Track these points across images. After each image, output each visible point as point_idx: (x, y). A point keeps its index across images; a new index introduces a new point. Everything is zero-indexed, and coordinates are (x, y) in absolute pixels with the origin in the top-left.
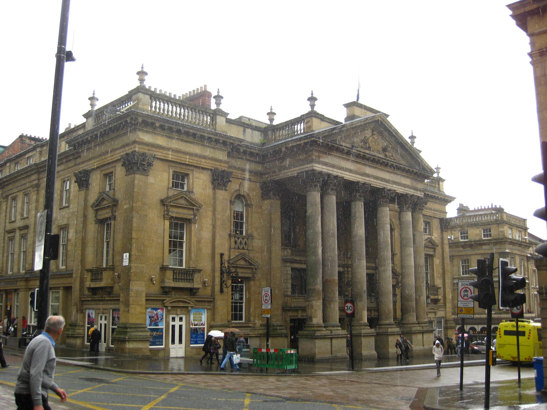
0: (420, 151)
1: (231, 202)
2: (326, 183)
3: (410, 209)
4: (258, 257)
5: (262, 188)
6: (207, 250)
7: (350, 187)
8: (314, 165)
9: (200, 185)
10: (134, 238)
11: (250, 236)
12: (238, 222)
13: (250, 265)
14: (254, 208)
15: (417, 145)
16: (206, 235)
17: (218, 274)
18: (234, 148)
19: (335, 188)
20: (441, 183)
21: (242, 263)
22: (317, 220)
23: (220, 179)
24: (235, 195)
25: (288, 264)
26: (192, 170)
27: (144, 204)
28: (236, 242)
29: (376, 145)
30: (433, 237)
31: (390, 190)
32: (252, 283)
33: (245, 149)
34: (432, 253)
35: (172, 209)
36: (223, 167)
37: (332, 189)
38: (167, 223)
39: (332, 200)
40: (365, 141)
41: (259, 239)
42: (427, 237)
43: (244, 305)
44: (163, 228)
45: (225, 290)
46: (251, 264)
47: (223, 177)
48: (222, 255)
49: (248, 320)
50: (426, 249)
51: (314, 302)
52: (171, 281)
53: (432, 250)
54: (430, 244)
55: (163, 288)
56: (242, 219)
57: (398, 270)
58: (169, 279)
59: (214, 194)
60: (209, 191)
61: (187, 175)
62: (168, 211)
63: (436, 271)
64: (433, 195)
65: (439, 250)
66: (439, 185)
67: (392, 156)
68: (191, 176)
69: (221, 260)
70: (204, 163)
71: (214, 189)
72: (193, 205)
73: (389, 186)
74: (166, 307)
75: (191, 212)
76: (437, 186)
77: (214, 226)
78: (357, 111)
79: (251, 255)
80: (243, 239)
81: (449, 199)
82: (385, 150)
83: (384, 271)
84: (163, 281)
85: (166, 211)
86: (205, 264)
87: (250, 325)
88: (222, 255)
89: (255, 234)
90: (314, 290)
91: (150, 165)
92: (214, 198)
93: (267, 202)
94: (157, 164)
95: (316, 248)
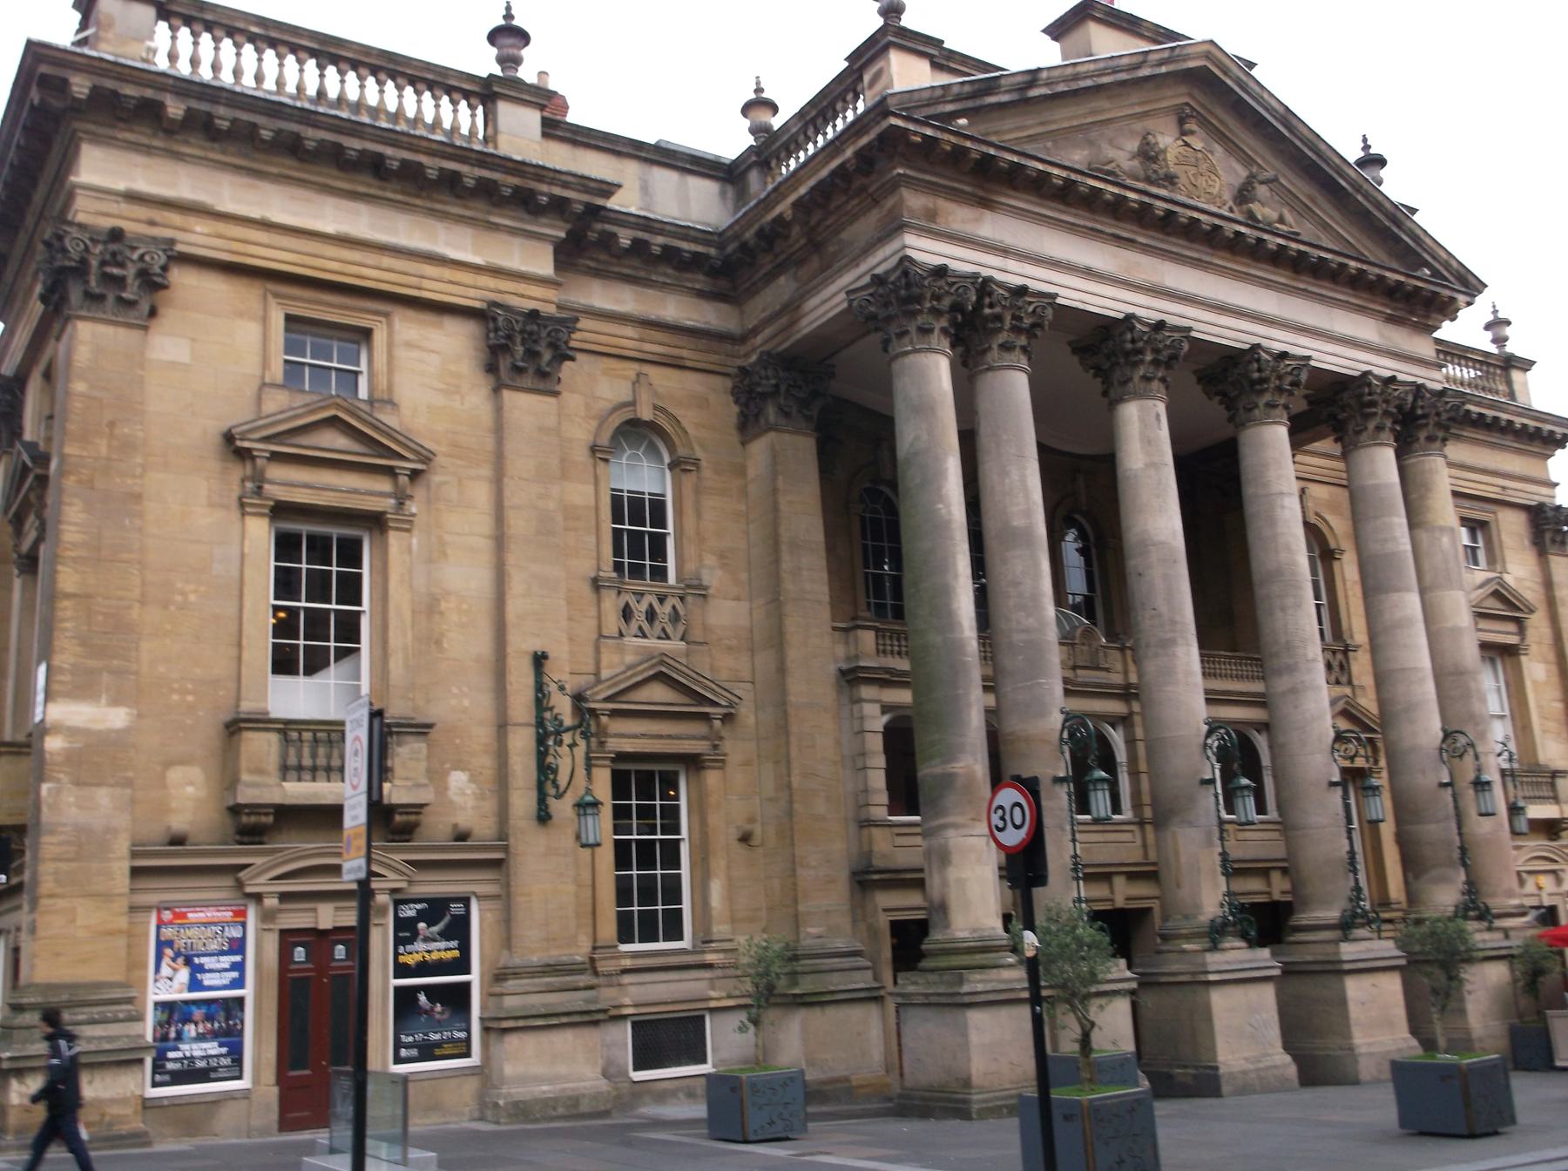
0: (1414, 211)
1: (593, 449)
2: (978, 321)
3: (1387, 436)
4: (724, 667)
5: (736, 393)
6: (467, 642)
7: (1103, 353)
8: (910, 239)
9: (425, 375)
10: (68, 596)
11: (695, 589)
12: (637, 535)
13: (697, 703)
14: (707, 472)
15: (1395, 186)
16: (466, 577)
17: (522, 742)
18: (589, 235)
19: (1023, 341)
20: (1516, 375)
21: (658, 694)
22: (940, 474)
23: (522, 349)
24: (616, 420)
25: (867, 692)
26: (386, 315)
27: (127, 447)
28: (627, 613)
29: (1210, 179)
30: (1508, 579)
31: (1284, 355)
32: (712, 778)
33: (640, 235)
34: (1513, 640)
35: (276, 472)
36: (541, 300)
37: (1007, 347)
38: (261, 534)
39: (1013, 390)
40: (1148, 154)
41: (737, 599)
42: (1480, 575)
43: (685, 871)
44: (235, 551)
45: (554, 805)
46: (702, 700)
47: (530, 338)
48: (539, 660)
49: (705, 940)
50: (1483, 624)
51: (951, 833)
52: (273, 779)
53: (1512, 627)
54: (1499, 606)
55: (235, 810)
56: (659, 520)
57: (1368, 702)
58: (260, 771)
59: (499, 410)
60: (475, 397)
61: (366, 334)
62: (259, 480)
63: (1540, 707)
64: (1490, 413)
65: (1538, 625)
66: (1509, 383)
67: (1281, 220)
68: (379, 337)
69: (540, 687)
70: (436, 285)
71: (497, 390)
72: (394, 459)
73: (1279, 340)
74: (258, 898)
75: (384, 485)
76: (1502, 387)
77: (500, 541)
78: (1107, 44)
79: (702, 663)
80: (662, 599)
81: (1559, 430)
82: (1243, 195)
83: (1294, 691)
84: (230, 780)
85: (253, 479)
86: (461, 703)
87: (710, 958)
88: (539, 660)
89: (713, 577)
90: (947, 780)
91: (153, 283)
92: (499, 429)
93: (760, 448)
94: (184, 280)
95: (945, 593)
